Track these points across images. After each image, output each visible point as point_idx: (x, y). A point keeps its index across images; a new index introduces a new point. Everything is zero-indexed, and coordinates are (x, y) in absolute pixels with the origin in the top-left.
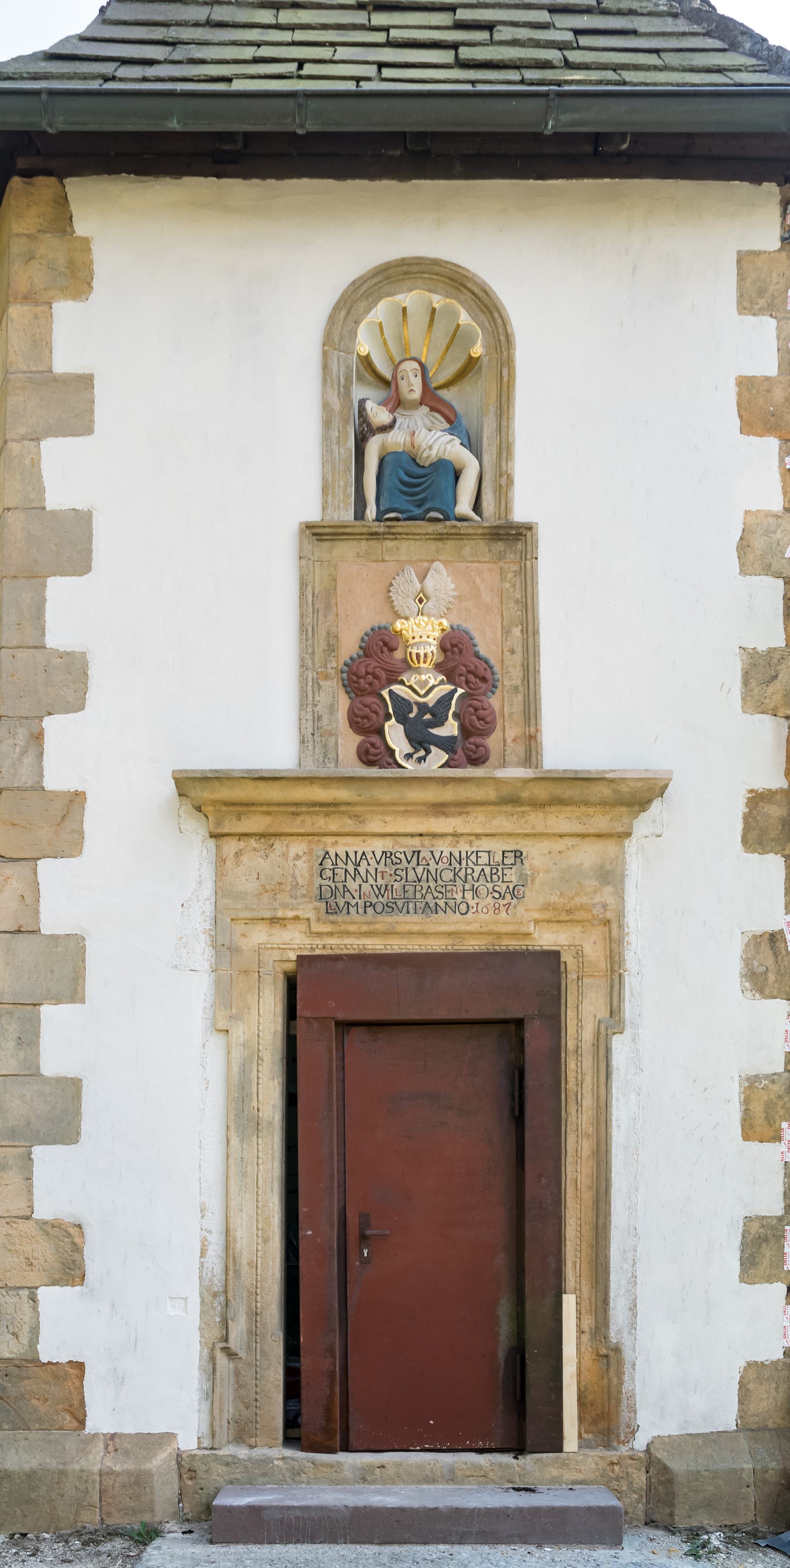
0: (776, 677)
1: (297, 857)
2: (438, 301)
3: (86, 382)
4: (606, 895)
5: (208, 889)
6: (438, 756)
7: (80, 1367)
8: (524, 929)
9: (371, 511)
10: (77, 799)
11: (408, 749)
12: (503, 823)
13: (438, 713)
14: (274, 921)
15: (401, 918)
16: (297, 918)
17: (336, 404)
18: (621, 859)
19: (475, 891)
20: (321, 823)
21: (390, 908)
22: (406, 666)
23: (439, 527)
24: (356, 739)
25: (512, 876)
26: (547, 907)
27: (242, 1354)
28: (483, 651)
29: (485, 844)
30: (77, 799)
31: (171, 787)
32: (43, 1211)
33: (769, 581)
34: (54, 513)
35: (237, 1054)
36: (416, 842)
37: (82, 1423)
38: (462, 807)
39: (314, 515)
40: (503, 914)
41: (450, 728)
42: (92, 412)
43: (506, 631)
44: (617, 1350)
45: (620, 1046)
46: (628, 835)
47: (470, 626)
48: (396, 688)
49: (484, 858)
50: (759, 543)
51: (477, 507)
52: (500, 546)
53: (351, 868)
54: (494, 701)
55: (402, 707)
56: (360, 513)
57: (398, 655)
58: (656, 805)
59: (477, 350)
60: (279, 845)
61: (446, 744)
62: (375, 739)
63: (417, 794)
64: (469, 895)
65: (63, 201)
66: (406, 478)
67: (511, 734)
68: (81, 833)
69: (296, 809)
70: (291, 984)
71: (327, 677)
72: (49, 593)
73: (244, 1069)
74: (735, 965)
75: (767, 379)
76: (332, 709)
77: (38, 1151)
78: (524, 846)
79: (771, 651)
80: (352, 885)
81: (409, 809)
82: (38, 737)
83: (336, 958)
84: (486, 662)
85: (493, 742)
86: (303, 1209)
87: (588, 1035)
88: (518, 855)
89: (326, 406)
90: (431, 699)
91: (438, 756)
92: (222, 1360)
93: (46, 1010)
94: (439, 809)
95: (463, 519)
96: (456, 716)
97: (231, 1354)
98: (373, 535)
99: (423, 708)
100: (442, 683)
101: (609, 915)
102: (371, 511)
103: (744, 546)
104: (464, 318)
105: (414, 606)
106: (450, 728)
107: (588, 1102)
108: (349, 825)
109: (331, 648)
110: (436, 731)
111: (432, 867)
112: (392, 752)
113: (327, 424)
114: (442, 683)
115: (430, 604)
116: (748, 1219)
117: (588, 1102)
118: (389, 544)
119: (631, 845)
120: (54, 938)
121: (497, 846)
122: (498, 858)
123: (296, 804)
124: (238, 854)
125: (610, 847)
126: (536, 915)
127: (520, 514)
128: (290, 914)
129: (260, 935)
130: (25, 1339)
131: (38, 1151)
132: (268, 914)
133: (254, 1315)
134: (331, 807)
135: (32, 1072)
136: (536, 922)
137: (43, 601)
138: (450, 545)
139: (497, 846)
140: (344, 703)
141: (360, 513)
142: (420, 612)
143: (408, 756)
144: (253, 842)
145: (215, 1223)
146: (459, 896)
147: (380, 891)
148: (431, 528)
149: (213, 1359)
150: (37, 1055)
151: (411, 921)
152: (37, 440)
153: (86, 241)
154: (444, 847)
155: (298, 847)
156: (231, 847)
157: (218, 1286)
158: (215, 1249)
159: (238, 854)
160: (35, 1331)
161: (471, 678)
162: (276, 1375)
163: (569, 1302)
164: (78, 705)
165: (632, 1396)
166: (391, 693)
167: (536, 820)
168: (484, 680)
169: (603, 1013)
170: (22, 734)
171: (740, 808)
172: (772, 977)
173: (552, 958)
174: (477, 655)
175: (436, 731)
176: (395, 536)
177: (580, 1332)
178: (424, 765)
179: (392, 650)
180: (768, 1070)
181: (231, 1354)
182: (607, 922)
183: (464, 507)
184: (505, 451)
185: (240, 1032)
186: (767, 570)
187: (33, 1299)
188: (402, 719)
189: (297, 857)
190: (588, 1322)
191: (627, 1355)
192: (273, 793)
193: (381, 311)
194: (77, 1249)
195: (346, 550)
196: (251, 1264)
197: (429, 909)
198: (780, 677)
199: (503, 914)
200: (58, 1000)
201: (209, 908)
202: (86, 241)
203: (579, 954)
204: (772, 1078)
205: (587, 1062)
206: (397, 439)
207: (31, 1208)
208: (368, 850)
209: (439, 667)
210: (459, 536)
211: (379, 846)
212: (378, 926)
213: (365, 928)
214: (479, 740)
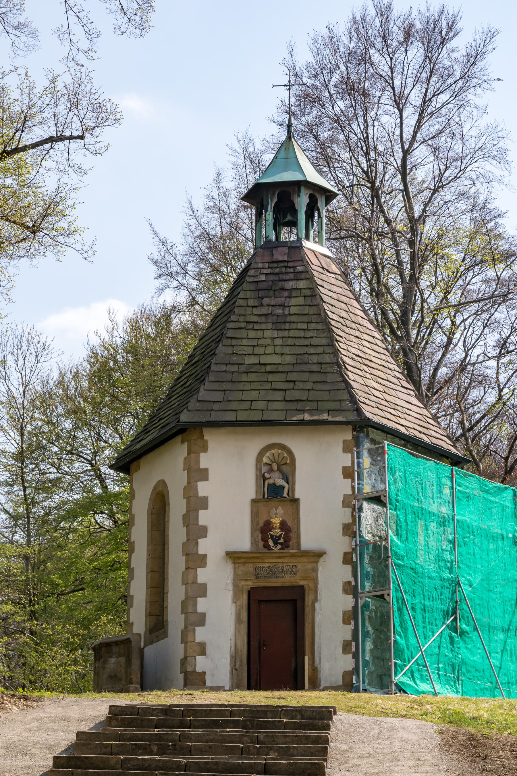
2: (280, 451)
3: (207, 470)
4: (314, 574)
5: (232, 574)
6: (279, 547)
7: (205, 673)
9: (266, 496)
10: (205, 556)
12: (292, 560)
13: (279, 537)
14: (246, 580)
17: (259, 474)
18: (317, 567)
20: (255, 560)
21: (269, 577)
22: (273, 528)
24: (263, 543)
25: (294, 570)
26: (301, 577)
28: (289, 524)
29: (289, 564)
30: (205, 556)
31: (225, 553)
32: (197, 640)
33: (348, 509)
35: (238, 607)
37: (205, 684)
38: (284, 557)
39: (253, 496)
41: (282, 541)
43: (294, 520)
44: (316, 668)
45: (317, 605)
47: (286, 520)
50: (346, 501)
51: (288, 494)
54: (291, 535)
55: (272, 536)
56: (264, 497)
58: (324, 556)
59: (288, 461)
60: (247, 565)
61: (281, 544)
69: (250, 558)
70: (249, 592)
73: (239, 610)
76: (258, 536)
77: (197, 628)
78: (297, 564)
81: (273, 558)
82: (197, 543)
83: (258, 587)
85: (291, 543)
86: (251, 639)
87: (310, 602)
88: (296, 566)
89: (257, 475)
90: (278, 535)
91: (279, 547)
92: (234, 670)
93: (199, 599)
94: (279, 557)
95: (285, 497)
97: (236, 669)
98: (266, 501)
99: (276, 536)
102: (266, 496)
103: (343, 502)
104: (285, 455)
106: (282, 541)
107: (310, 616)
108: (261, 561)
109: (258, 524)
113: (257, 479)
116: (344, 641)
117: (310, 616)
119: (320, 564)
120: (200, 584)
121: (292, 564)
125: (315, 564)
127: (297, 496)
129: (243, 583)
131: (197, 628)
133: (241, 661)
135: (195, 611)
139: (292, 564)
140: (260, 535)
141: (264, 497)
145: (233, 642)
147: (267, 574)
149: (232, 671)
151: (274, 580)
154: (280, 565)
155: (251, 565)
156: (237, 565)
157: (234, 655)
158: (233, 648)
160: (195, 665)
162: (245, 674)
163: (306, 658)
164: (205, 536)
165: (320, 678)
167: (299, 559)
169: (313, 598)
170: (194, 543)
171: (342, 556)
173: (303, 587)
177: (309, 664)
180: (348, 610)
181: (236, 669)
183: (285, 495)
184: (294, 483)
185: (239, 603)
186: (348, 507)
187: (195, 659)
188: (272, 539)
190: (310, 662)
191: (319, 669)
192: (246, 555)
193: (268, 454)
194: (205, 648)
195: (261, 504)
196: (241, 651)
200: (201, 597)
201: (232, 577)
203: (309, 586)
204: (349, 611)
205: (310, 608)
206: (271, 481)
209: (280, 528)
210: (284, 501)
211: (267, 565)
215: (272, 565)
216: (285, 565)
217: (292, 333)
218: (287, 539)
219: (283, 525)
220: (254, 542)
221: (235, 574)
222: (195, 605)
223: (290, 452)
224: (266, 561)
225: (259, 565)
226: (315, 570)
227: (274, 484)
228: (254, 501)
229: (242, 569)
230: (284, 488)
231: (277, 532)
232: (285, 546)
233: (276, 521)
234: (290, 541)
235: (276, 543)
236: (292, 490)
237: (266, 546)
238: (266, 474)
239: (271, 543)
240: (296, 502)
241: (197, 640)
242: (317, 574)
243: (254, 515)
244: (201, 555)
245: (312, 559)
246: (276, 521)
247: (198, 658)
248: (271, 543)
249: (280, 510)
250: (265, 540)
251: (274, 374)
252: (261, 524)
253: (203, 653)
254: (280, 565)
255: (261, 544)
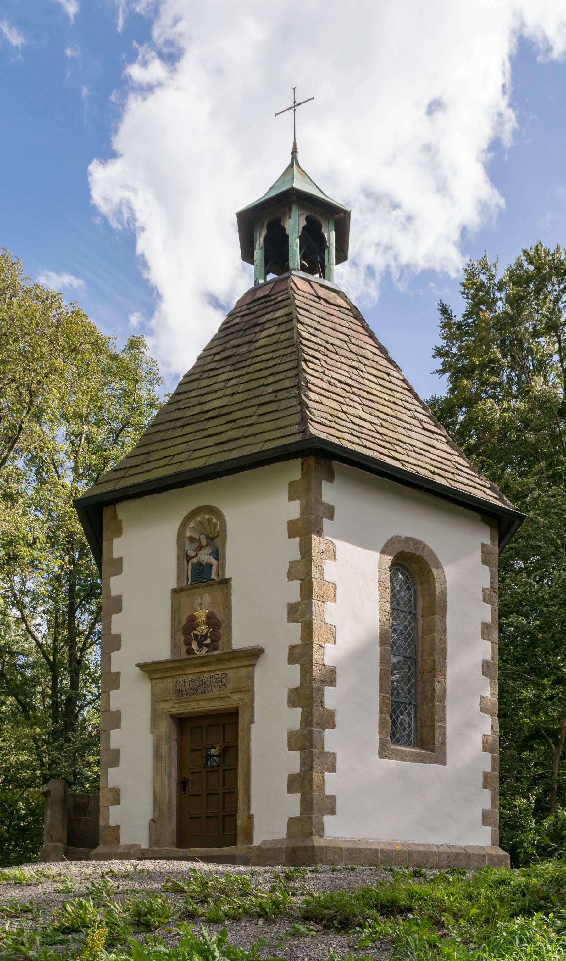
0: (297, 611)
1: (170, 683)
6: (205, 649)
7: (118, 827)
8: (227, 695)
10: (118, 674)
11: (198, 648)
12: (221, 666)
14: (165, 701)
15: (196, 696)
16: (170, 699)
19: (214, 686)
21: (193, 694)
22: (198, 625)
23: (206, 584)
25: (224, 681)
27: (157, 821)
28: (218, 617)
29: (217, 673)
30: (118, 674)
32: (110, 786)
34: (113, 597)
36: (199, 675)
37: (119, 842)
39: (174, 586)
40: (222, 692)
42: (122, 567)
46: (255, 665)
47: (214, 610)
48: (195, 632)
49: (217, 676)
52: (222, 586)
53: (183, 684)
54: (221, 631)
55: (196, 636)
57: (196, 622)
60: (166, 680)
61: (208, 646)
62: (189, 647)
63: (195, 662)
64: (213, 688)
65: (115, 511)
66: (198, 571)
67: (225, 639)
68: (119, 683)
71: (178, 631)
72: (112, 619)
74: (286, 699)
75: (296, 520)
76: (180, 640)
77: (110, 770)
79: (296, 603)
80: (184, 689)
84: (218, 620)
85: (220, 643)
88: (226, 674)
89: (178, 556)
91: (205, 649)
96: (210, 637)
99: (202, 636)
100: (207, 628)
101: (250, 688)
105: (199, 607)
106: (208, 641)
108: (182, 672)
110: (204, 642)
111: (203, 681)
112: (193, 650)
114: (207, 628)
115: (203, 607)
118: (194, 591)
120: (114, 712)
121: (220, 673)
122: (220, 676)
123: (168, 668)
124: (156, 684)
125: (250, 669)
126: (231, 691)
127: (227, 576)
128: (169, 698)
129: (162, 705)
130: (106, 821)
131: (110, 770)
132: (163, 699)
134: (176, 668)
135: (109, 748)
136: (231, 693)
137: (111, 621)
138: (209, 588)
140: (183, 638)
142: (201, 609)
143: (198, 651)
144: (159, 680)
146: (210, 688)
147: (191, 689)
148: (204, 584)
150: (110, 743)
152: (109, 578)
153: (121, 520)
155: (170, 680)
156: (154, 682)
159: (156, 684)
161: (213, 626)
164: (118, 648)
166: (194, 633)
167: (229, 665)
168: (217, 625)
172: (296, 701)
174: (216, 618)
175: (204, 642)
176: (195, 588)
178: (202, 652)
179: (194, 621)
182: (249, 690)
183: (213, 576)
187: (108, 809)
188: (196, 640)
189: (170, 683)
194: (119, 795)
195: (183, 594)
196: (160, 796)
197: (203, 693)
198: (299, 610)
199: (222, 692)
202: (121, 520)
207: (108, 784)
208: (187, 678)
209: (206, 624)
210: (212, 585)
212: (191, 699)
213: (187, 700)
214: (215, 643)
215: (196, 677)
216: (212, 674)
217: (252, 369)
218: (216, 639)
219: (211, 619)
220: (174, 647)
221: (153, 694)
222: (108, 740)
223: (220, 516)
224: (188, 672)
225: (180, 679)
226: (251, 677)
227: (200, 564)
228: (175, 592)
229: (161, 685)
230: (211, 566)
231: (202, 629)
232: (213, 647)
233: (201, 615)
234: (218, 641)
235: (201, 646)
236: (222, 567)
237: (190, 651)
238: (189, 552)
239: (194, 645)
240: (225, 583)
241: (110, 786)
242: (253, 682)
243: (175, 610)
244: (114, 673)
245: (246, 663)
246: (201, 615)
247: (111, 807)
248: (194, 645)
249: (207, 599)
250: (188, 643)
251: (216, 419)
252: (184, 621)
253: (117, 801)
254: (206, 675)
255: (184, 648)
